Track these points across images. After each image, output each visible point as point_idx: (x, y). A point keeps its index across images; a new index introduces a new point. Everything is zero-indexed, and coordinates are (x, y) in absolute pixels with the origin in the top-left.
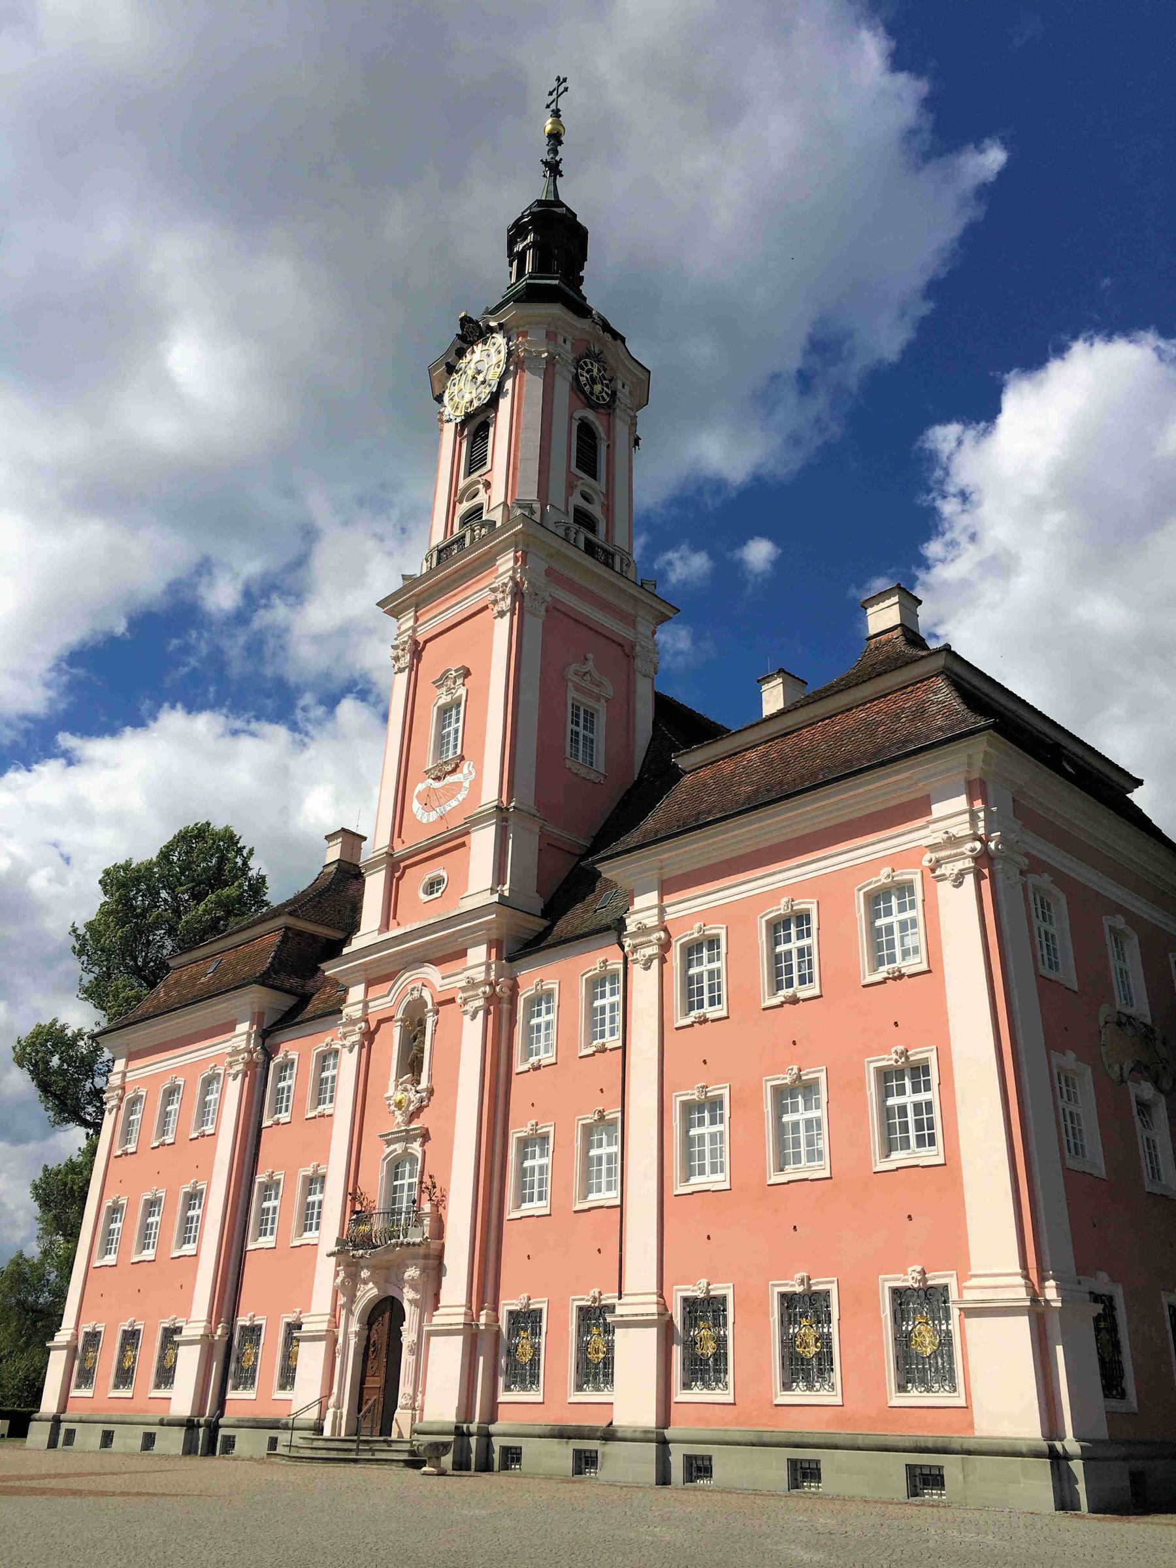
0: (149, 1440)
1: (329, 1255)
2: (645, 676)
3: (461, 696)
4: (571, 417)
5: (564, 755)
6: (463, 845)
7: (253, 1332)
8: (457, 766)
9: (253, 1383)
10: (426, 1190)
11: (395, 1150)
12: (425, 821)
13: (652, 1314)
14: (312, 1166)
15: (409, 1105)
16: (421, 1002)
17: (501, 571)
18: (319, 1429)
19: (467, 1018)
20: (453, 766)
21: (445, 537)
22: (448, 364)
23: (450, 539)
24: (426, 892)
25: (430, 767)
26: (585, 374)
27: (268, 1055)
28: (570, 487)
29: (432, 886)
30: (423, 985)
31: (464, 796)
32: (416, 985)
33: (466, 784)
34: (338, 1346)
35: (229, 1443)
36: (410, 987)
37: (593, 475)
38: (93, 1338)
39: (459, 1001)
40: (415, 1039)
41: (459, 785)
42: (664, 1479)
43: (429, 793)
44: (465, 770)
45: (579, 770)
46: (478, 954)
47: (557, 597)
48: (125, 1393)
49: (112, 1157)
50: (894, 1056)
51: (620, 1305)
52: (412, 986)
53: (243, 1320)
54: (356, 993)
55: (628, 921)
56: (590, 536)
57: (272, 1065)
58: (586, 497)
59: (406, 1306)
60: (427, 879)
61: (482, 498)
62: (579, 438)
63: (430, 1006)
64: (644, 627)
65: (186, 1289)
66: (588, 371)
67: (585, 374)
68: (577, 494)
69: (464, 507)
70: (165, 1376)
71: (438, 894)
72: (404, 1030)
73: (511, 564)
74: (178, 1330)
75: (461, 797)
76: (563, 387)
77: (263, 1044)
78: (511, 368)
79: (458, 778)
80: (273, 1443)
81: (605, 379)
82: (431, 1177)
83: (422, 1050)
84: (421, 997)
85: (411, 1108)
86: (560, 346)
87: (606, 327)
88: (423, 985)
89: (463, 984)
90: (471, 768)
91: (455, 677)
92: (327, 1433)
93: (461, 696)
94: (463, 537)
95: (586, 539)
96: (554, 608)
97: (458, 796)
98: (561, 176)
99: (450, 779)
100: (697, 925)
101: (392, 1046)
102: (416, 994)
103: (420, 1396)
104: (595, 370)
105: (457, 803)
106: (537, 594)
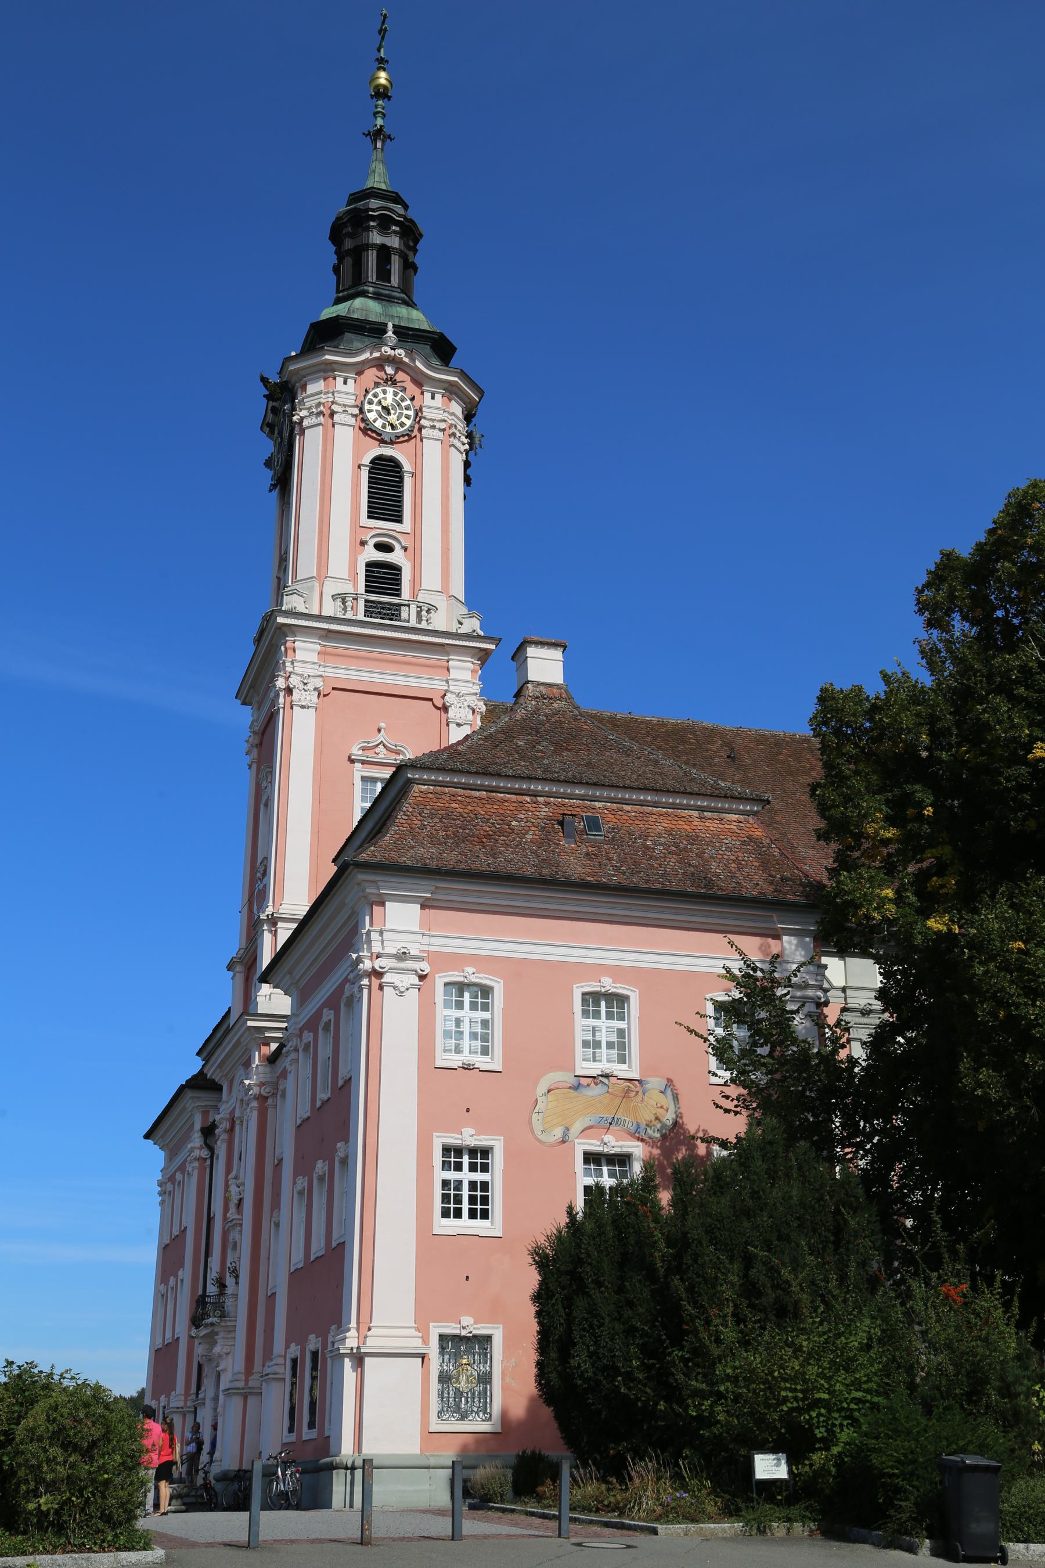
4: (359, 467)
68: (370, 548)
96: (334, 689)
106: (305, 684)
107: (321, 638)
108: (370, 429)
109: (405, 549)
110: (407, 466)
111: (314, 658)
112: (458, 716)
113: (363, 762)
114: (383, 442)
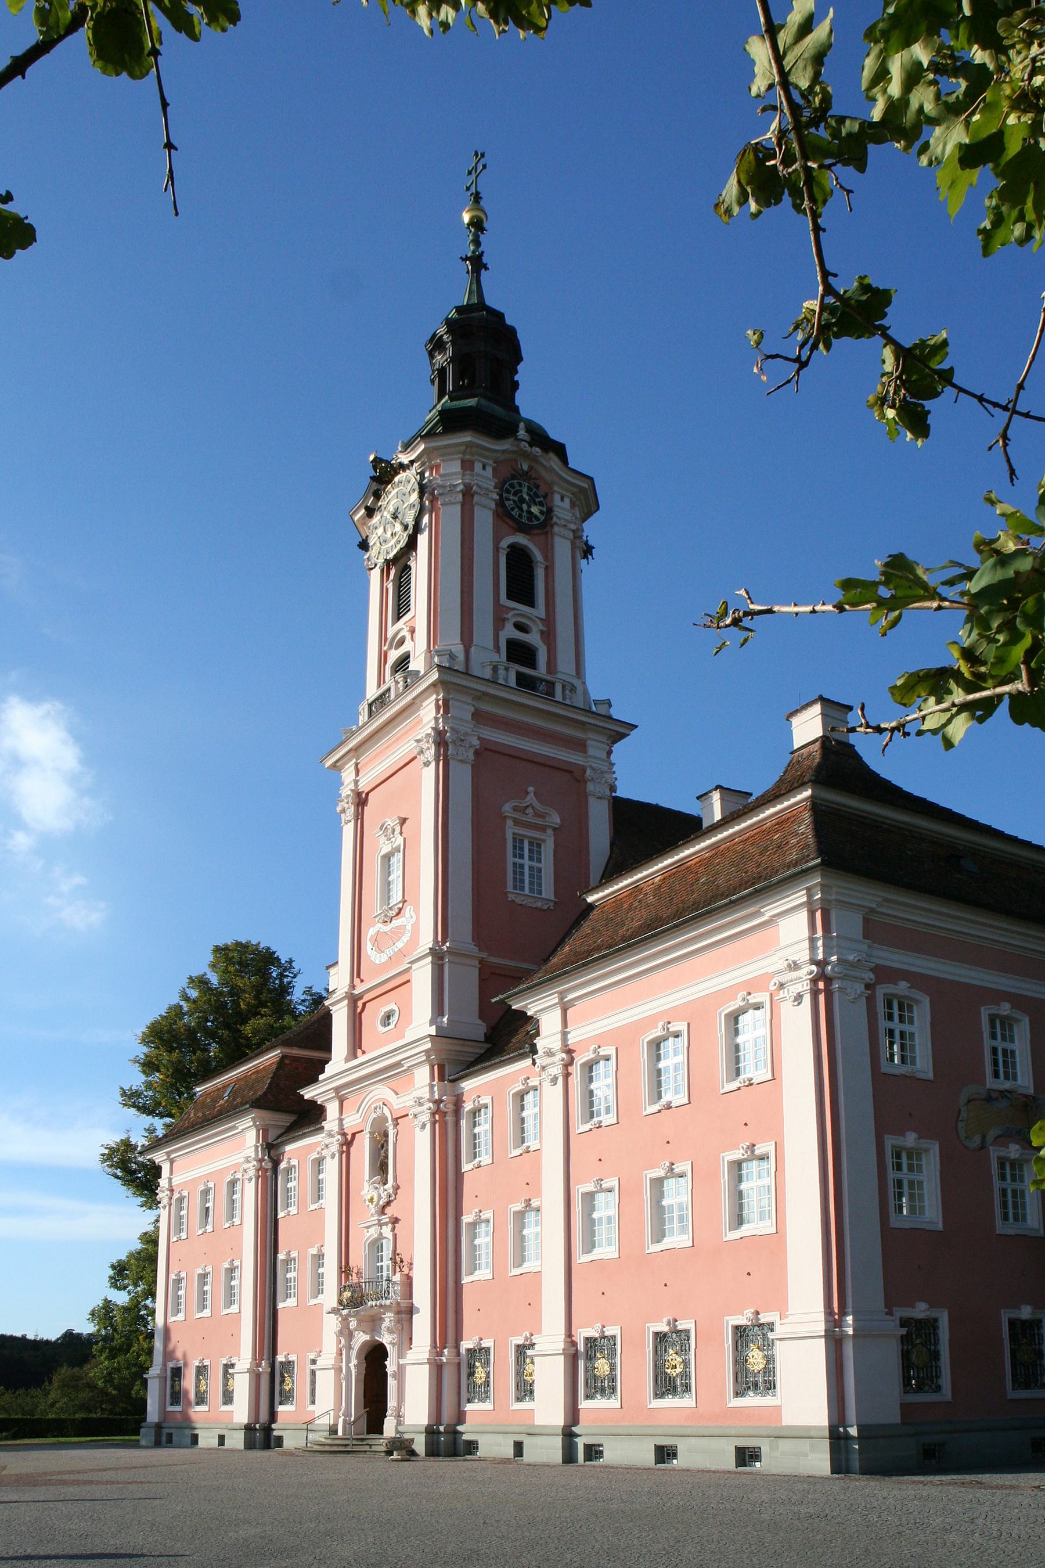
4: (496, 550)
6: (408, 981)
8: (400, 910)
11: (372, 1235)
15: (379, 1201)
18: (333, 1430)
19: (418, 1130)
25: (379, 912)
26: (512, 497)
28: (499, 622)
29: (388, 1016)
30: (384, 1104)
31: (408, 938)
36: (373, 1106)
40: (382, 1148)
41: (403, 928)
44: (407, 915)
46: (423, 1076)
47: (484, 736)
59: (388, 1347)
60: (383, 1014)
66: (515, 494)
67: (512, 497)
71: (392, 1026)
72: (373, 1139)
75: (405, 938)
81: (538, 497)
83: (387, 1157)
85: (381, 1203)
87: (539, 438)
88: (384, 1104)
92: (340, 1433)
97: (403, 938)
102: (379, 1111)
104: (525, 490)
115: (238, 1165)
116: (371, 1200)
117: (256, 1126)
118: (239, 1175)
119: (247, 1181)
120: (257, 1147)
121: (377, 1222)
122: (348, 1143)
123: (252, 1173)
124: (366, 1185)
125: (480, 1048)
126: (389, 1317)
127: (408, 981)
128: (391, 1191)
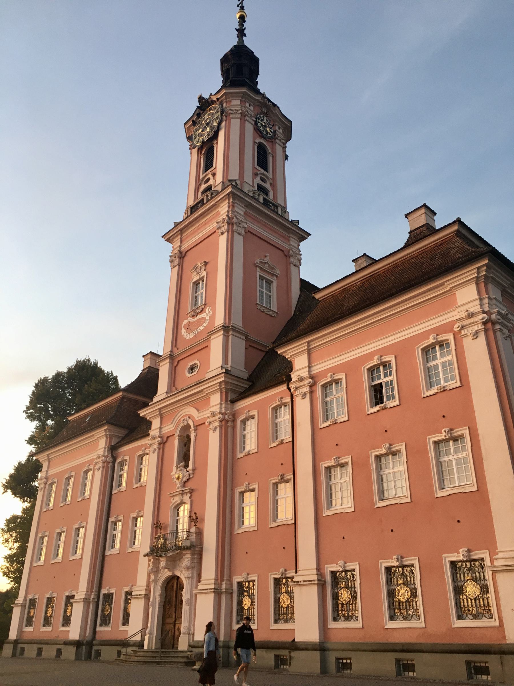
0: (59, 652)
1: (145, 556)
2: (295, 266)
3: (204, 277)
4: (254, 142)
5: (257, 301)
6: (207, 346)
7: (109, 597)
8: (203, 309)
9: (110, 623)
10: (193, 520)
11: (177, 501)
12: (188, 338)
13: (314, 580)
14: (136, 512)
16: (188, 427)
17: (221, 213)
20: (201, 310)
21: (194, 201)
22: (193, 121)
23: (197, 201)
24: (189, 373)
27: (114, 458)
29: (192, 368)
30: (189, 418)
31: (206, 324)
32: (185, 418)
33: (208, 318)
34: (150, 602)
35: (98, 654)
36: (182, 420)
37: (266, 170)
38: (33, 603)
39: (207, 424)
41: (204, 319)
42: (324, 670)
43: (189, 323)
44: (207, 311)
45: (264, 310)
46: (216, 399)
48: (49, 629)
49: (42, 512)
50: (444, 434)
51: (296, 576)
52: (184, 419)
53: (104, 591)
54: (156, 424)
55: (292, 376)
56: (265, 197)
57: (117, 462)
58: (262, 180)
60: (189, 366)
61: (211, 182)
62: (258, 152)
63: (192, 428)
64: (293, 242)
65: (77, 575)
69: (203, 187)
70: (67, 620)
71: (196, 373)
73: (227, 209)
74: (73, 597)
75: (205, 325)
76: (249, 128)
77: (112, 452)
78: (224, 118)
79: (204, 316)
80: (119, 653)
82: (195, 513)
84: (188, 423)
85: (184, 479)
86: (247, 107)
89: (209, 415)
90: (210, 310)
91: (201, 267)
92: (146, 647)
93: (204, 277)
94: (203, 199)
95: (264, 199)
96: (249, 231)
98: (245, 36)
99: (200, 316)
100: (329, 375)
101: (174, 450)
102: (186, 423)
103: (192, 627)
105: (203, 328)
106: (240, 224)
107: (246, 206)
108: (258, 129)
109: (271, 184)
110: (270, 151)
111: (243, 214)
112: (294, 262)
113: (261, 269)
114: (262, 136)
115: (93, 460)
116: (178, 478)
117: (106, 435)
118: (91, 467)
119: (96, 470)
120: (105, 448)
121: (181, 492)
122: (164, 442)
123: (100, 465)
124: (174, 468)
125: (247, 385)
126: (188, 558)
127: (207, 346)
128: (191, 472)
